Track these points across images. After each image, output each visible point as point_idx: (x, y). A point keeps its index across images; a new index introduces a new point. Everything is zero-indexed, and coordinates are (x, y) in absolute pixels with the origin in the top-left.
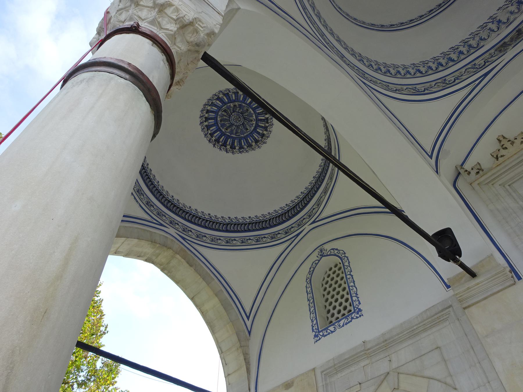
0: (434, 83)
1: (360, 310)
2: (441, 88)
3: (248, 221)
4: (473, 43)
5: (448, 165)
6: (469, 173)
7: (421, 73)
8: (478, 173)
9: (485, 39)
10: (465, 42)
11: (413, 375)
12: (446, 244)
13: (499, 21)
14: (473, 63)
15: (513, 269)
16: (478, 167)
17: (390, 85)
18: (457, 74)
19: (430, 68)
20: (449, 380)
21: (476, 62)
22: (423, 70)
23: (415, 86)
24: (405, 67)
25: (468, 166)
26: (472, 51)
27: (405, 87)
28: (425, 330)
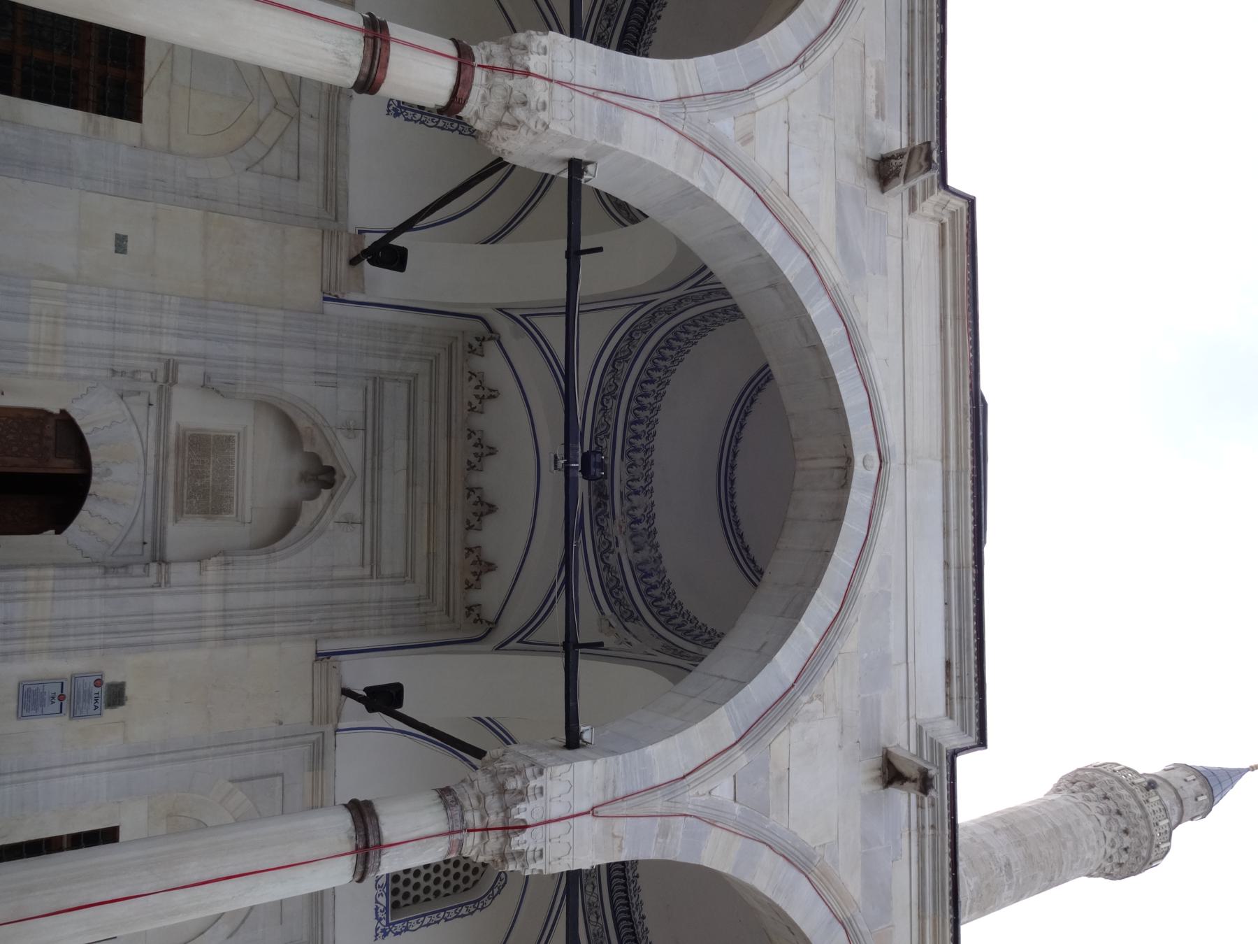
0: (620, 384)
1: (397, 115)
2: (604, 385)
3: (654, 11)
4: (638, 456)
5: (503, 325)
6: (477, 339)
7: (646, 382)
8: (470, 346)
9: (630, 466)
10: (649, 450)
11: (281, 135)
12: (388, 255)
13: (637, 493)
14: (611, 437)
15: (337, 300)
16: (479, 351)
17: (644, 337)
18: (613, 415)
19: (646, 395)
20: (258, 168)
21: (610, 441)
22: (649, 387)
23: (630, 362)
24: (667, 370)
25: (491, 347)
26: (627, 447)
27: (635, 351)
28: (326, 178)
